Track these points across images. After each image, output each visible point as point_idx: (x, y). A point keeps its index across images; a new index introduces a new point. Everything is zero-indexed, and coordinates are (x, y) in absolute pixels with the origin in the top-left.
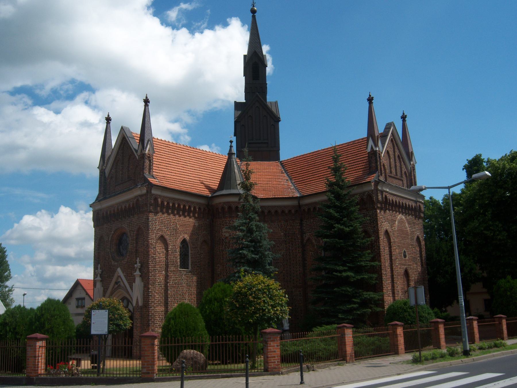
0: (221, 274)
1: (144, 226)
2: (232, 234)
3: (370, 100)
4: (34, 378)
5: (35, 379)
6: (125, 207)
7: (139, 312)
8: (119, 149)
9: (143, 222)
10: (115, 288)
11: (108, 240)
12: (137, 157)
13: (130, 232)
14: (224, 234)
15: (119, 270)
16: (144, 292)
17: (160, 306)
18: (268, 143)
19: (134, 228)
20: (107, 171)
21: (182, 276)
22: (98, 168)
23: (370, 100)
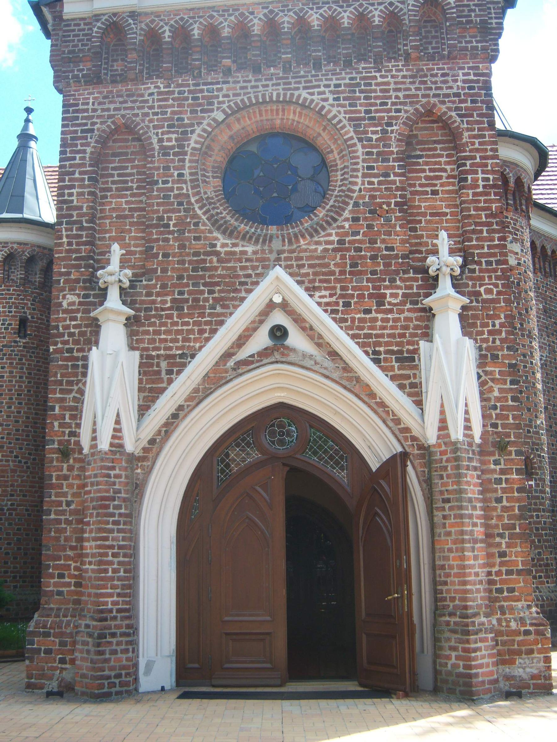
1: (457, 109)
9: (457, 95)
11: (181, 146)
16: (482, 384)
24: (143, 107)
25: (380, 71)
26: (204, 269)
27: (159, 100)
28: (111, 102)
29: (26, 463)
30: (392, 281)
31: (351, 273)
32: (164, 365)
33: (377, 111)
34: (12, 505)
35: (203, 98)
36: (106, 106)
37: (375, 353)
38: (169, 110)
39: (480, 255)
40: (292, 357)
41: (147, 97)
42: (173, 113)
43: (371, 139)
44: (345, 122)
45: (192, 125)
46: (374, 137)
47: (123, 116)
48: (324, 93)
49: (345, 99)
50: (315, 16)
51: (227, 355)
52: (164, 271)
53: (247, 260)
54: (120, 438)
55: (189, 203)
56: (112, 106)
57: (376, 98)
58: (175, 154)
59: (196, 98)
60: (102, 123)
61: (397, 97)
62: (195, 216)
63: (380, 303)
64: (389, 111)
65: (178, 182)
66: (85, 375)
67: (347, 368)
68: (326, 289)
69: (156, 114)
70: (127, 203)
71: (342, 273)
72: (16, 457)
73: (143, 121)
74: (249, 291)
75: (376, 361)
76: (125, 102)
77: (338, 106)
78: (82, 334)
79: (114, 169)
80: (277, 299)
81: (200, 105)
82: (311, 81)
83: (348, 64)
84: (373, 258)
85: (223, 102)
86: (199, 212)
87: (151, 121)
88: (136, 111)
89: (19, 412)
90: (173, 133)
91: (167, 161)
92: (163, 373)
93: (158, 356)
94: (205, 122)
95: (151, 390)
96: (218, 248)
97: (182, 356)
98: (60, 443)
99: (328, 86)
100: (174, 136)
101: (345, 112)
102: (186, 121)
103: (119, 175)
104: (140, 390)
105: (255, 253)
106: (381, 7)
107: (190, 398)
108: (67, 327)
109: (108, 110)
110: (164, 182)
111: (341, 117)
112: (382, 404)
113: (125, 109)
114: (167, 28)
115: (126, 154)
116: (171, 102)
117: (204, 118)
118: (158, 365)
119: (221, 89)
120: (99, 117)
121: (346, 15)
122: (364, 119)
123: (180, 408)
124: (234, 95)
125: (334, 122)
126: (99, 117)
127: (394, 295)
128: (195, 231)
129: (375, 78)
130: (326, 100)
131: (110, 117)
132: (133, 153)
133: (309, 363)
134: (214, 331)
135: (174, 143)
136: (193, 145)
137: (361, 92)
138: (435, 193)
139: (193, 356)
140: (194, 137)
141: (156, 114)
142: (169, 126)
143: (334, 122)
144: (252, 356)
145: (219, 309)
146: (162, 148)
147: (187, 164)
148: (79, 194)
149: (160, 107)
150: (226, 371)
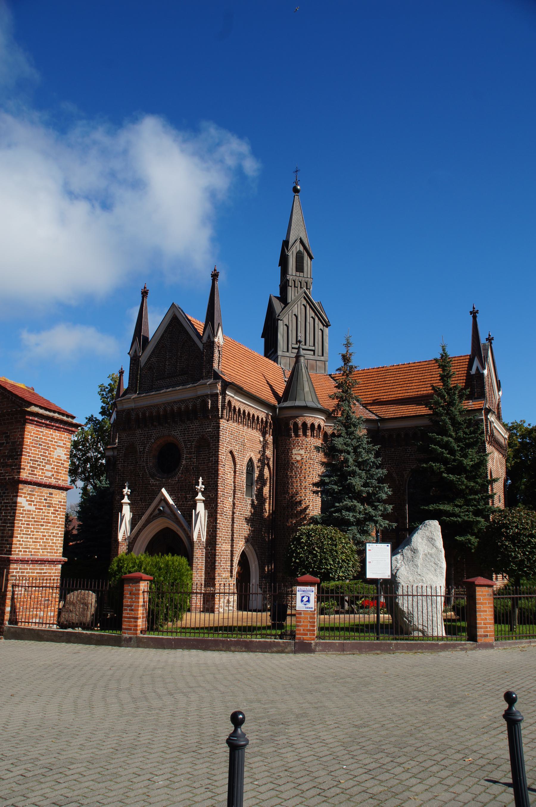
0: (288, 508)
1: (210, 436)
2: (305, 457)
3: (474, 314)
4: (312, 642)
5: (313, 644)
6: (180, 408)
7: (201, 549)
8: (165, 332)
10: (154, 514)
11: (144, 451)
12: (201, 346)
14: (294, 457)
15: (164, 490)
17: (226, 543)
18: (314, 351)
19: (193, 437)
20: (143, 360)
21: (247, 506)
22: (129, 353)
23: (474, 314)
37: (184, 514)
39: (212, 484)
51: (151, 514)
62: (146, 473)
63: (186, 499)
64: (193, 437)
80: (163, 498)
84: (185, 485)
107: (142, 526)
123: (140, 529)
134: (148, 507)
140: (147, 448)
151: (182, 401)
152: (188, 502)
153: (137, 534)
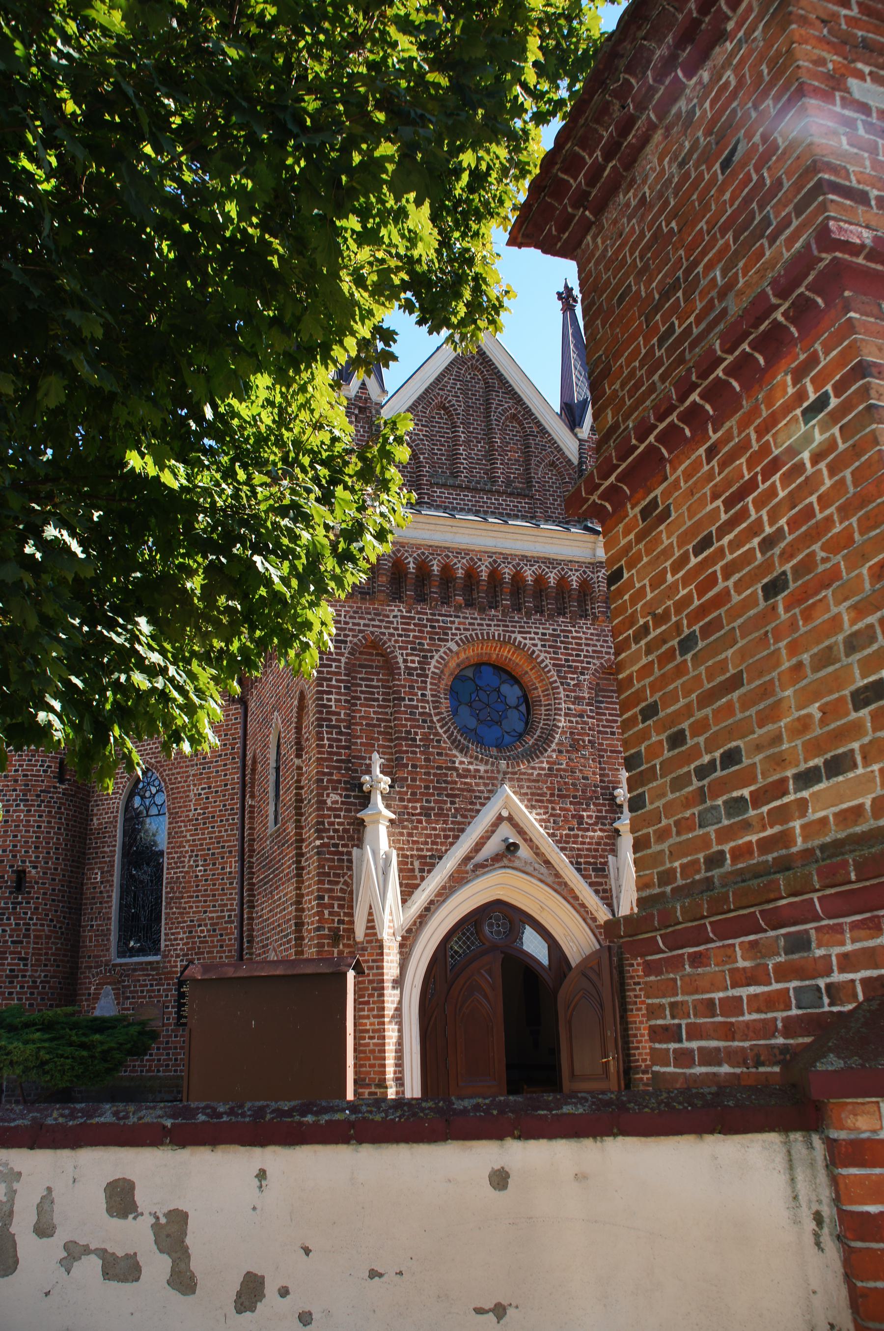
13: (558, 671)
24: (389, 628)
25: (574, 626)
26: (446, 782)
27: (402, 623)
28: (360, 618)
29: (61, 928)
30: (588, 805)
31: (558, 796)
32: (417, 864)
33: (573, 661)
34: (46, 976)
35: (440, 627)
36: (357, 621)
37: (578, 863)
38: (412, 634)
40: (517, 864)
41: (391, 619)
42: (415, 637)
43: (568, 684)
44: (550, 667)
45: (431, 651)
46: (572, 683)
47: (372, 633)
48: (533, 639)
49: (550, 647)
50: (529, 572)
51: (467, 859)
52: (414, 780)
53: (481, 777)
54: (373, 928)
55: (432, 721)
56: (362, 622)
57: (573, 649)
58: (418, 675)
59: (432, 627)
60: (354, 636)
61: (587, 651)
62: (437, 734)
63: (580, 823)
64: (582, 662)
65: (422, 701)
66: (350, 868)
67: (557, 875)
68: (540, 807)
69: (400, 635)
70: (375, 713)
71: (552, 795)
72: (52, 920)
73: (390, 640)
74: (483, 805)
75: (579, 870)
76: (373, 620)
77: (546, 652)
78: (346, 831)
79: (362, 679)
80: (505, 814)
81: (437, 633)
82: (523, 627)
83: (551, 617)
84: (574, 784)
85: (456, 635)
86: (441, 731)
87: (396, 641)
88: (383, 630)
89: (56, 869)
90: (416, 655)
91: (412, 681)
92: (417, 871)
93: (412, 856)
94: (442, 650)
95: (407, 885)
96: (457, 765)
97: (432, 857)
98: (330, 929)
99: (536, 633)
100: (417, 659)
101: (551, 658)
102: (426, 647)
103: (366, 686)
104: (401, 885)
105: (486, 771)
106: (577, 574)
107: (439, 894)
108: (332, 824)
109: (359, 624)
110: (411, 700)
111: (547, 661)
112: (583, 905)
113: (374, 626)
114: (410, 559)
115: (371, 667)
116: (412, 627)
117: (440, 646)
118: (412, 864)
119: (453, 622)
120: (350, 630)
121: (552, 575)
122: (563, 666)
123: (432, 902)
124: (465, 629)
125: (543, 665)
126: (350, 630)
127: (590, 817)
128: (438, 747)
129: (571, 632)
130: (535, 645)
131: (360, 631)
132: (377, 667)
133: (529, 869)
134: (457, 837)
135: (417, 665)
136: (432, 669)
137: (562, 642)
138: (613, 733)
139: (440, 858)
140: (434, 662)
141: (400, 635)
142: (412, 649)
143: (543, 665)
144: (487, 860)
145: (459, 818)
146: (407, 667)
147: (429, 687)
148: (337, 700)
149: (403, 629)
150: (467, 873)
151: (551, 562)
152: (587, 830)
153: (421, 916)
